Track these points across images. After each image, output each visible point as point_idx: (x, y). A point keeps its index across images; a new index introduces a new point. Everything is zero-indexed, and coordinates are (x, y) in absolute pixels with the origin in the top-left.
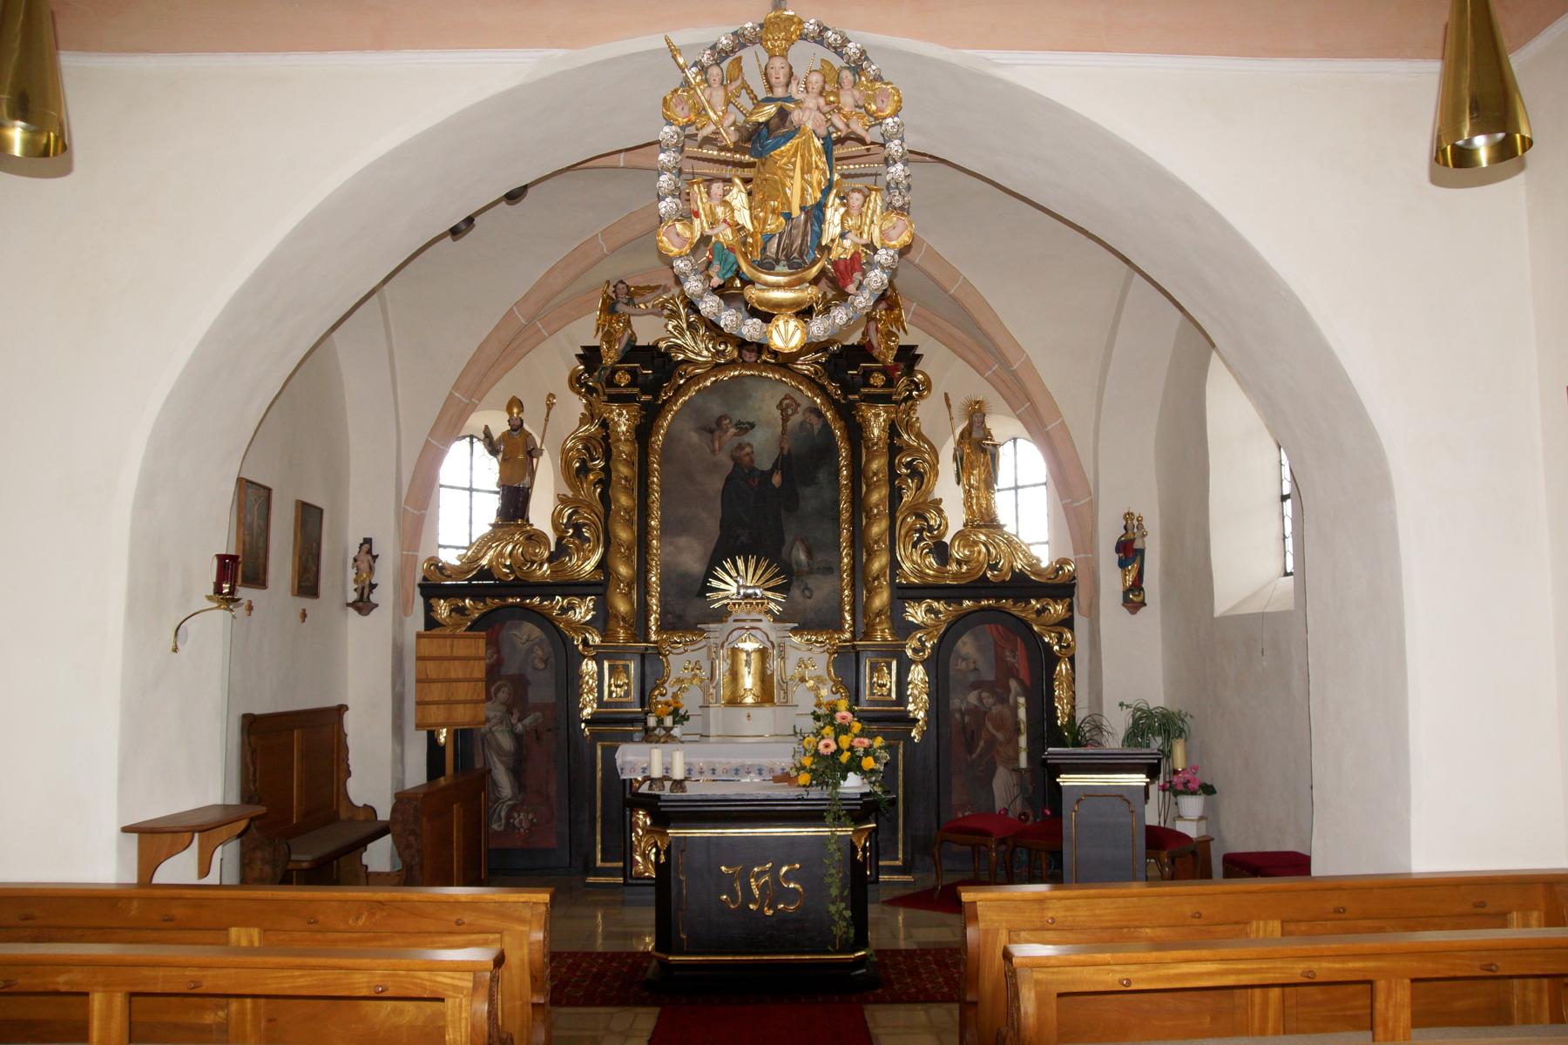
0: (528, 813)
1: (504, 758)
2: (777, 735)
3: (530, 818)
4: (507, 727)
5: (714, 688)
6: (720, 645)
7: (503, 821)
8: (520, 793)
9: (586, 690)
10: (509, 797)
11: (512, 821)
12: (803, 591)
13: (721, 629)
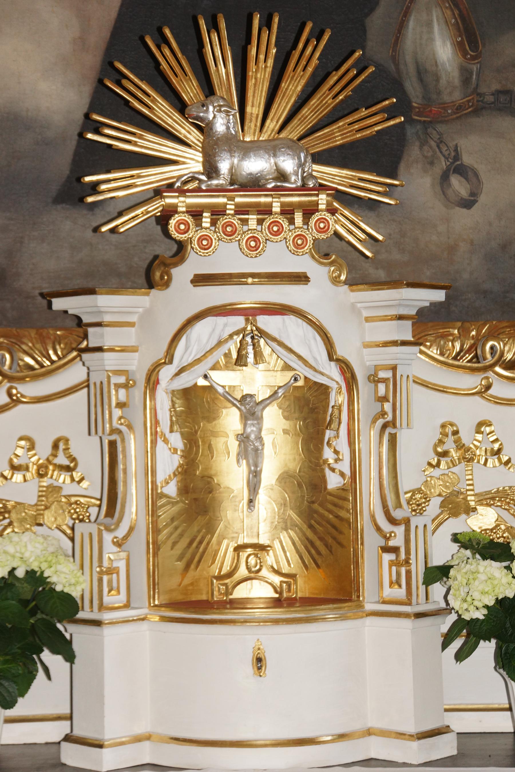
2: (369, 732)
5: (119, 544)
6: (141, 378)
12: (445, 177)
13: (148, 313)
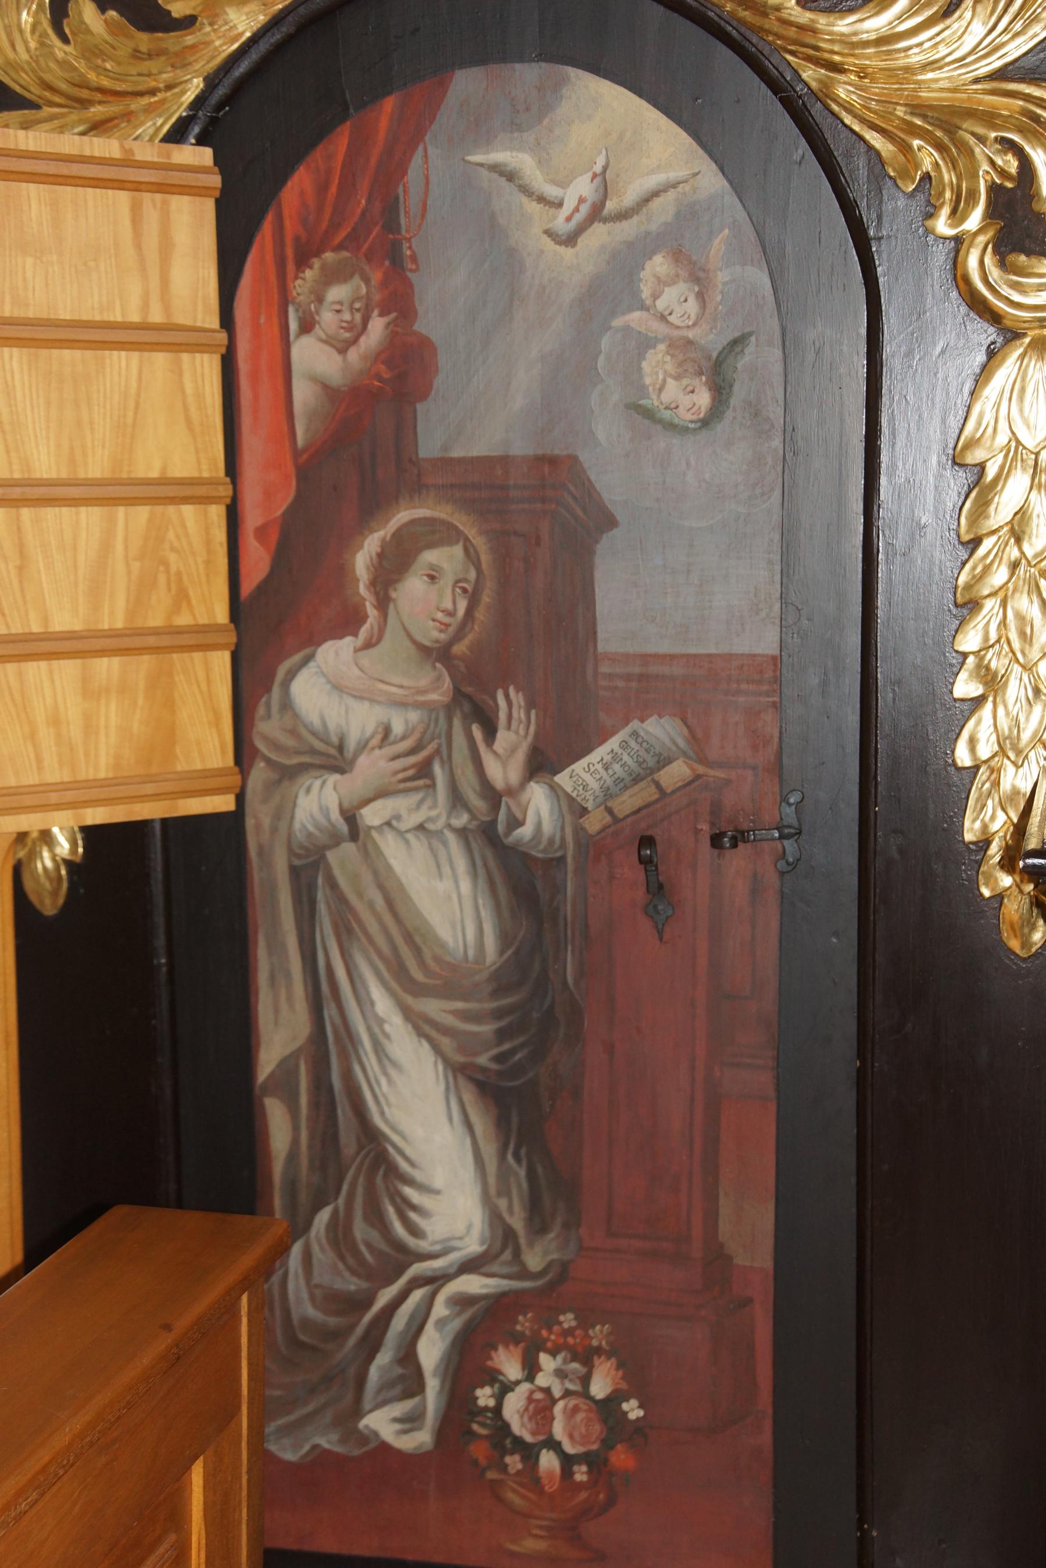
0: (586, 1357)
1: (434, 1008)
3: (600, 1388)
4: (457, 800)
7: (432, 1385)
8: (538, 1224)
9: (1000, 576)
10: (473, 1247)
11: (485, 1396)
